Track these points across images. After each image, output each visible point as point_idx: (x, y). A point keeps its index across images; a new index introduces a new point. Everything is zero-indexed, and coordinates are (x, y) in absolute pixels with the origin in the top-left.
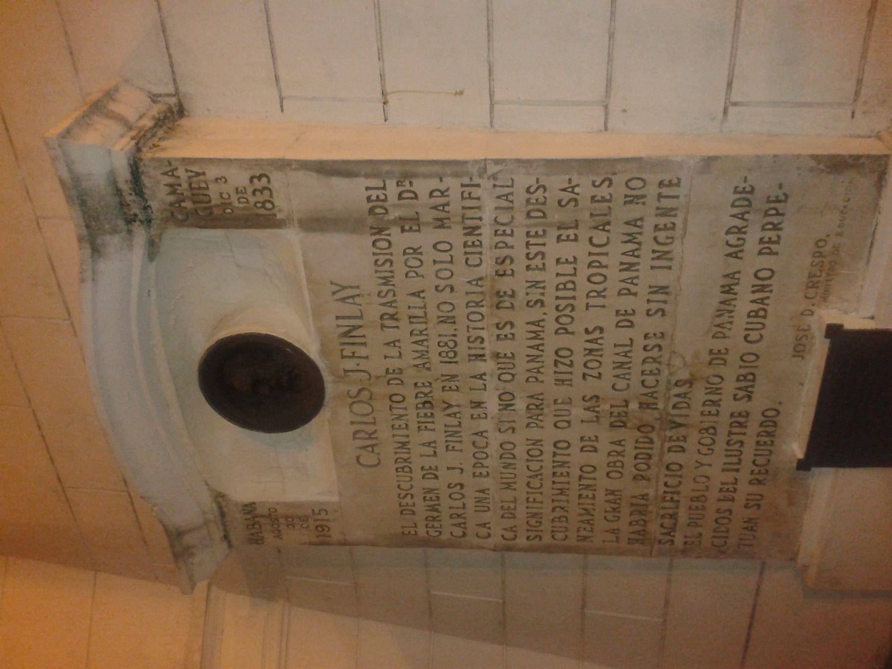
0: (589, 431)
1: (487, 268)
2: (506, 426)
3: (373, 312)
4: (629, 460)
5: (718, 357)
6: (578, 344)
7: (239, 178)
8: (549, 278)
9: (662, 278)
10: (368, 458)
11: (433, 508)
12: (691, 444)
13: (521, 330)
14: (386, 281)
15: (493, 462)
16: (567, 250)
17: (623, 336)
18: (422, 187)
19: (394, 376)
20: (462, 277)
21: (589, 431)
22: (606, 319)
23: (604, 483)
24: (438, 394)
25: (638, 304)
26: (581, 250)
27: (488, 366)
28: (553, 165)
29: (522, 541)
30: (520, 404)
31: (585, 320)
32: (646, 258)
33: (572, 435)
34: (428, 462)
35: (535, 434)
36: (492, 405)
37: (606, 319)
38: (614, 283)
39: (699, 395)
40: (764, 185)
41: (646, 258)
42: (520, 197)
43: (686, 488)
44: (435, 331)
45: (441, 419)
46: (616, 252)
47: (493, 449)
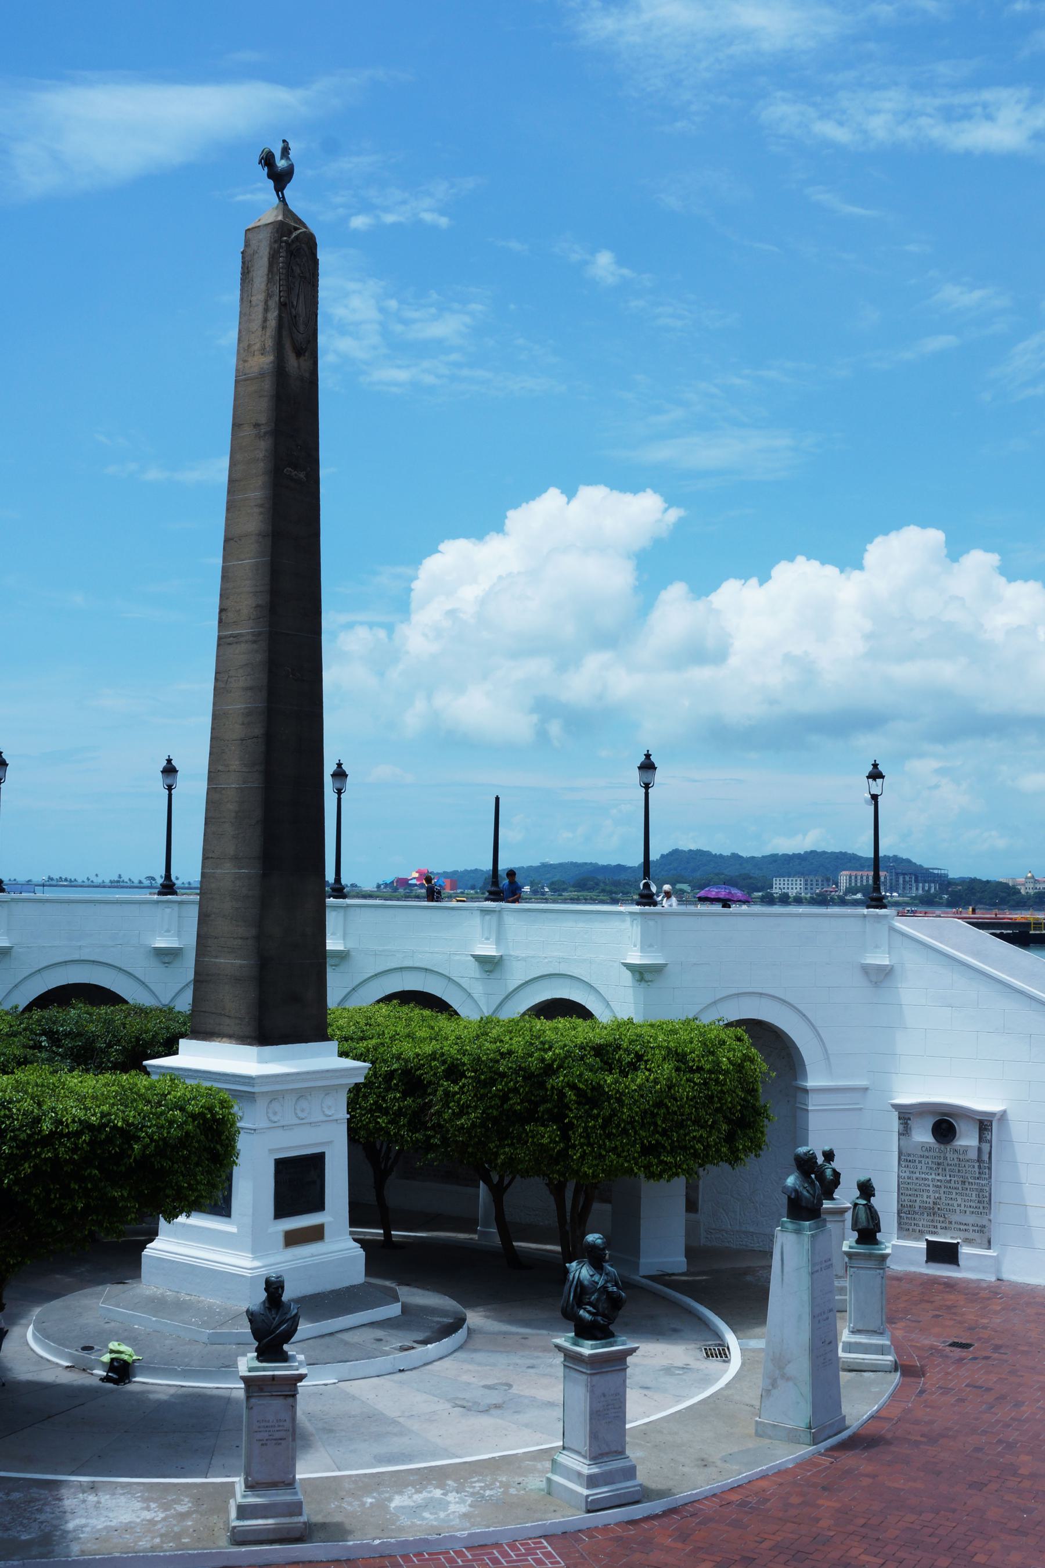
0: (932, 1197)
1: (970, 1181)
2: (933, 1180)
3: (961, 1157)
4: (925, 1205)
5: (951, 1223)
6: (954, 1196)
7: (989, 1137)
8: (968, 1192)
9: (968, 1212)
10: (924, 1149)
11: (910, 1161)
12: (929, 1218)
13: (956, 1185)
14: (968, 1161)
15: (923, 1176)
16: (974, 1195)
17: (955, 1205)
18: (987, 1171)
19: (946, 1158)
20: (969, 1176)
21: (932, 1197)
22: (959, 1202)
23: (918, 1199)
24: (941, 1167)
25: (963, 1208)
26: (974, 1198)
27: (948, 1178)
28: (990, 1195)
29: (901, 1180)
30: (939, 1183)
31: (959, 1198)
32: (972, 1210)
33: (931, 1193)
34: (923, 1162)
35: (931, 1186)
36: (938, 1178)
37: (959, 1202)
38: (966, 1204)
39: (942, 1219)
40: (985, 1230)
41: (972, 1210)
42: (984, 1188)
43: (917, 1216)
44: (957, 1168)
45: (935, 1167)
46: (972, 1204)
47: (927, 1176)
